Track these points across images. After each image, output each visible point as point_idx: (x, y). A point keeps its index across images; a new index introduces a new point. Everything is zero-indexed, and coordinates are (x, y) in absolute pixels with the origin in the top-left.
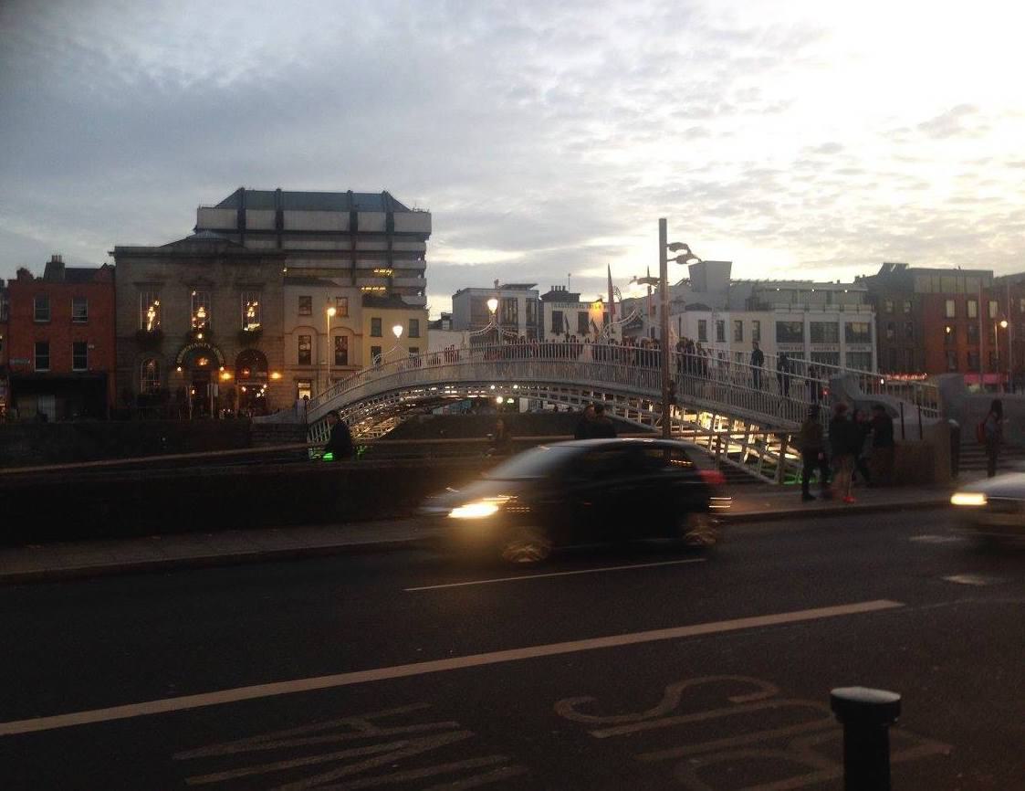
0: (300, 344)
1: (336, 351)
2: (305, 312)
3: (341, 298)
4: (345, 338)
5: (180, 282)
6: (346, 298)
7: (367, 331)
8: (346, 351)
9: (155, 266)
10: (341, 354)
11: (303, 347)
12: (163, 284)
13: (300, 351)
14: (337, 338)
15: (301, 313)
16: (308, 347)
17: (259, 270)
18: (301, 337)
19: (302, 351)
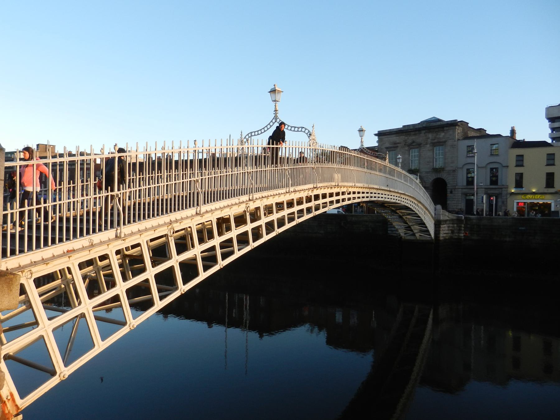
0: (467, 173)
1: (491, 177)
2: (471, 155)
3: (494, 144)
4: (497, 169)
5: (405, 145)
6: (498, 144)
7: (512, 162)
8: (497, 177)
9: (394, 138)
10: (494, 179)
11: (469, 175)
12: (397, 147)
13: (467, 177)
14: (492, 169)
15: (468, 155)
16: (473, 175)
17: (443, 134)
18: (468, 170)
19: (469, 177)
